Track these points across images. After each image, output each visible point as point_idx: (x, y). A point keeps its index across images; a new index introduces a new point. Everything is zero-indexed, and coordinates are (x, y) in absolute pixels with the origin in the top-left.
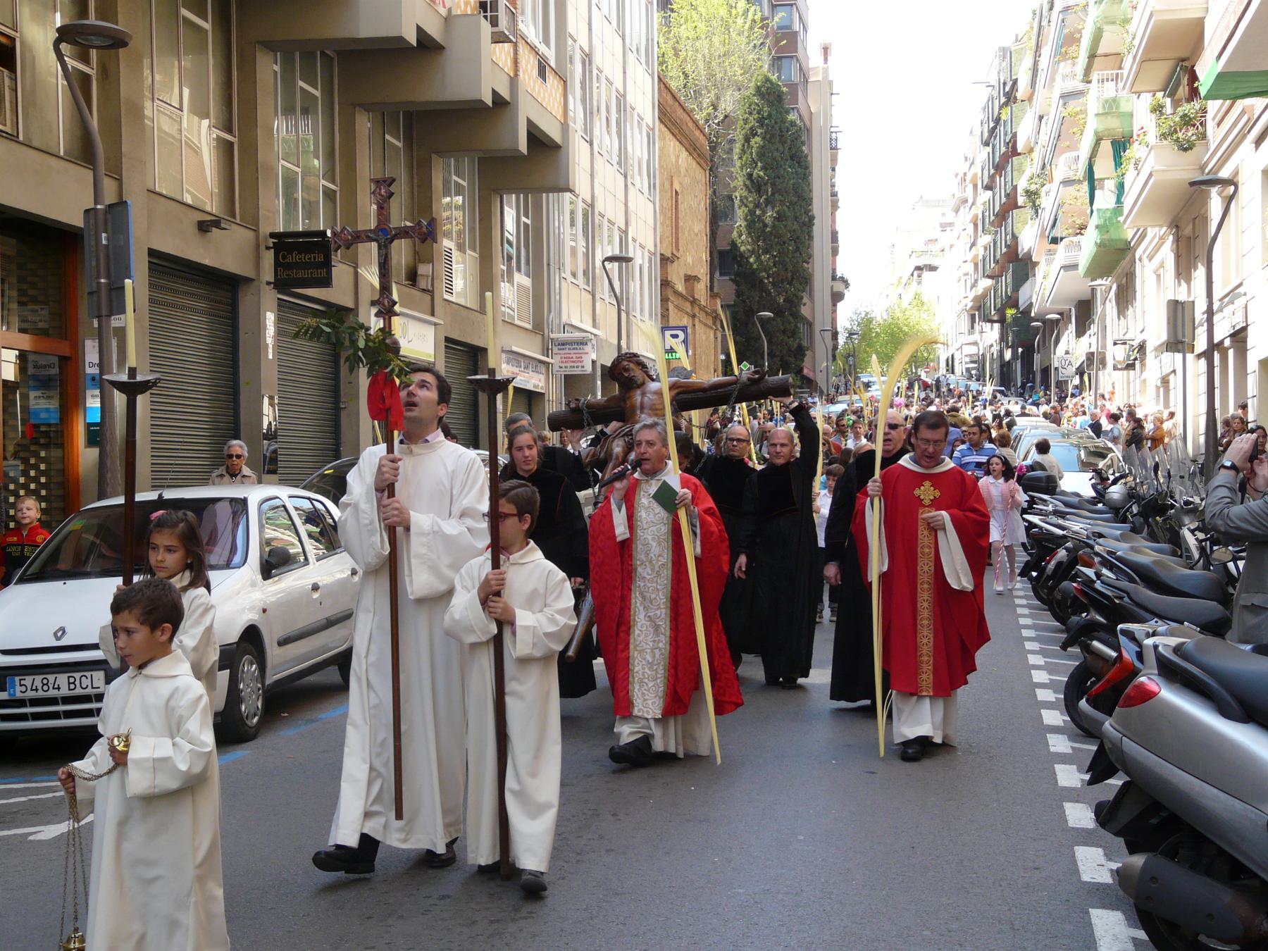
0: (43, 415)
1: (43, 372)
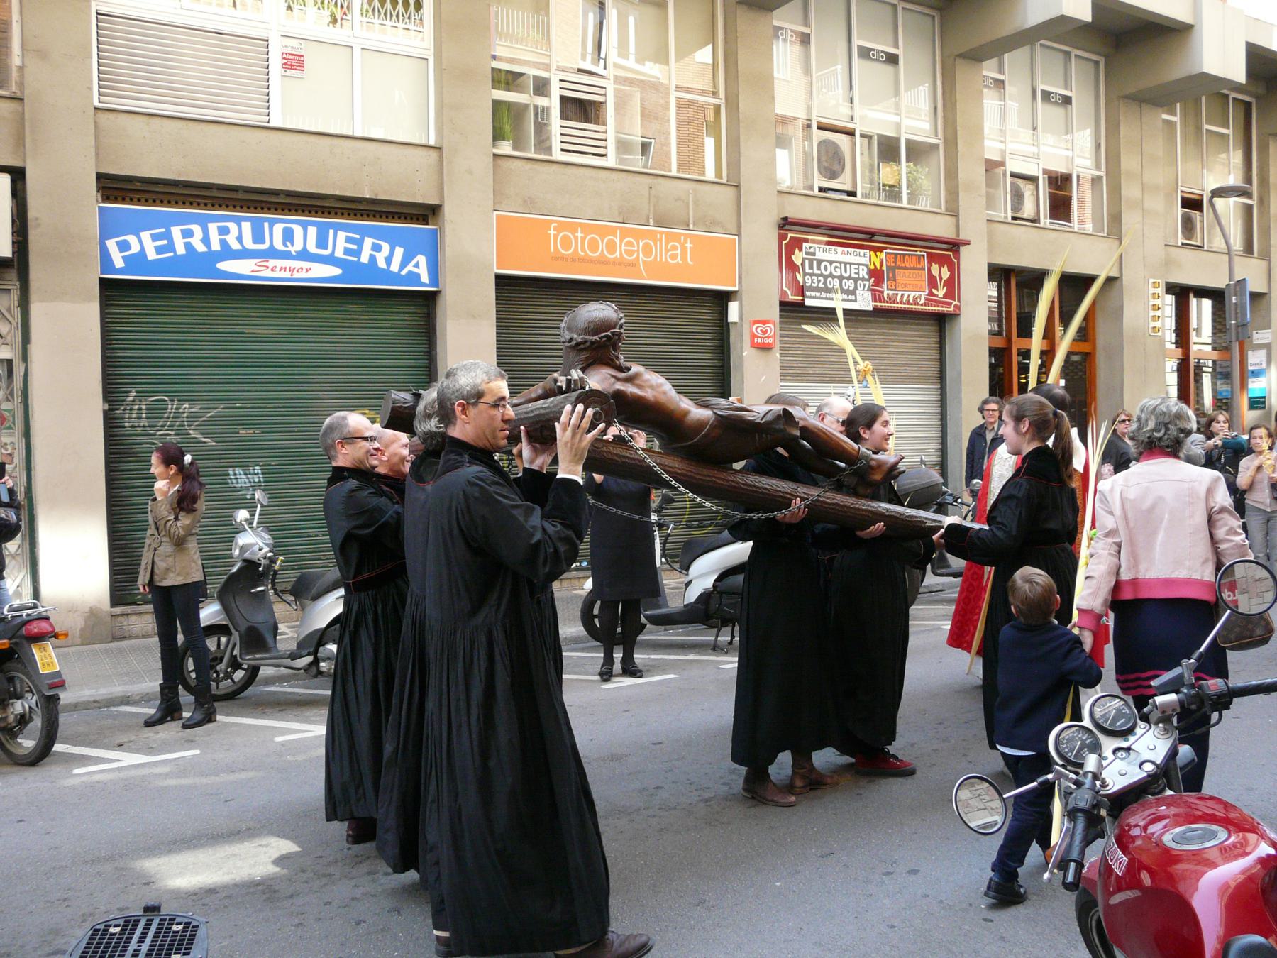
0: (1224, 394)
1: (1224, 370)
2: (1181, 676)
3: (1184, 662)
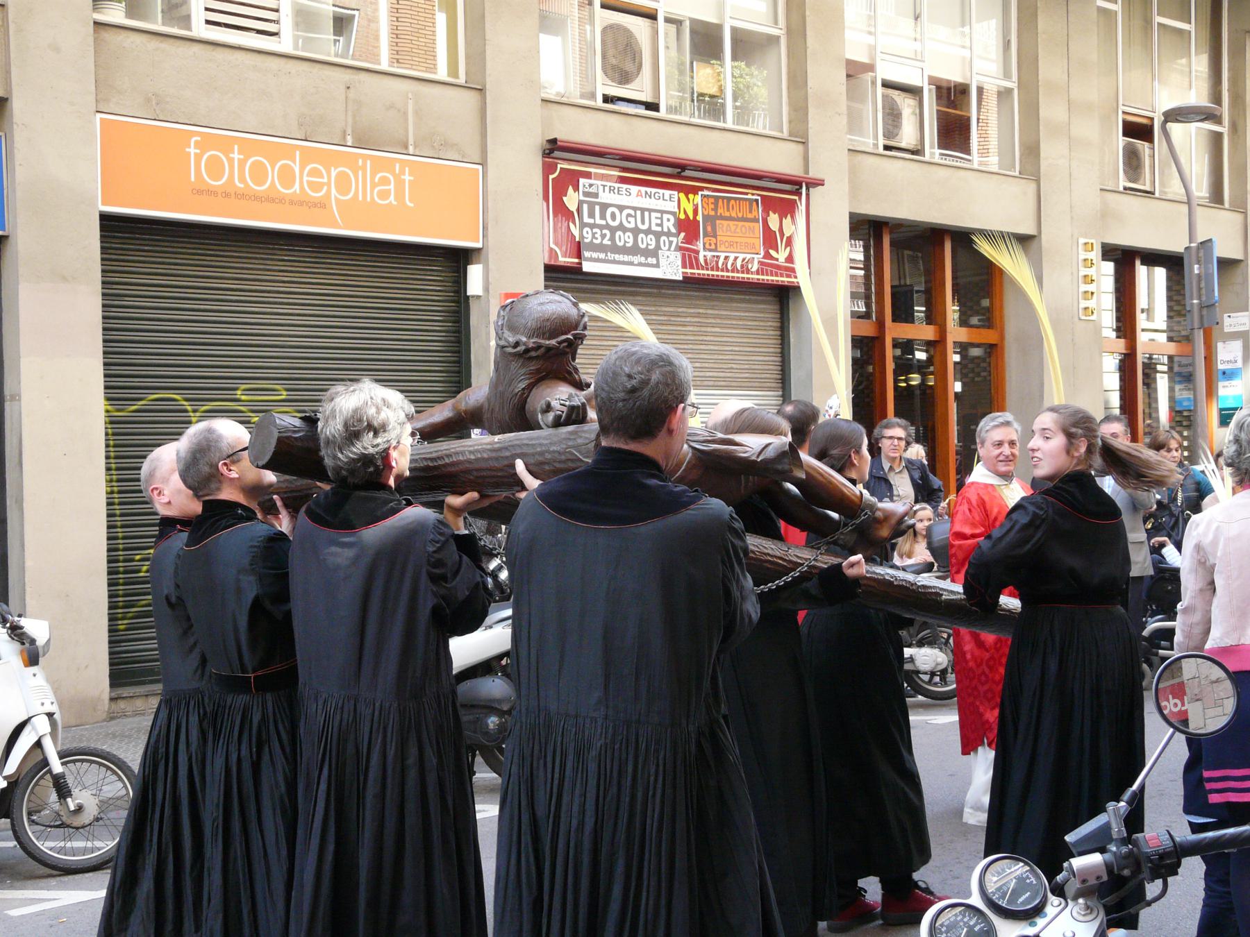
0: (1185, 404)
1: (1185, 370)
2: (1106, 828)
3: (1111, 806)
